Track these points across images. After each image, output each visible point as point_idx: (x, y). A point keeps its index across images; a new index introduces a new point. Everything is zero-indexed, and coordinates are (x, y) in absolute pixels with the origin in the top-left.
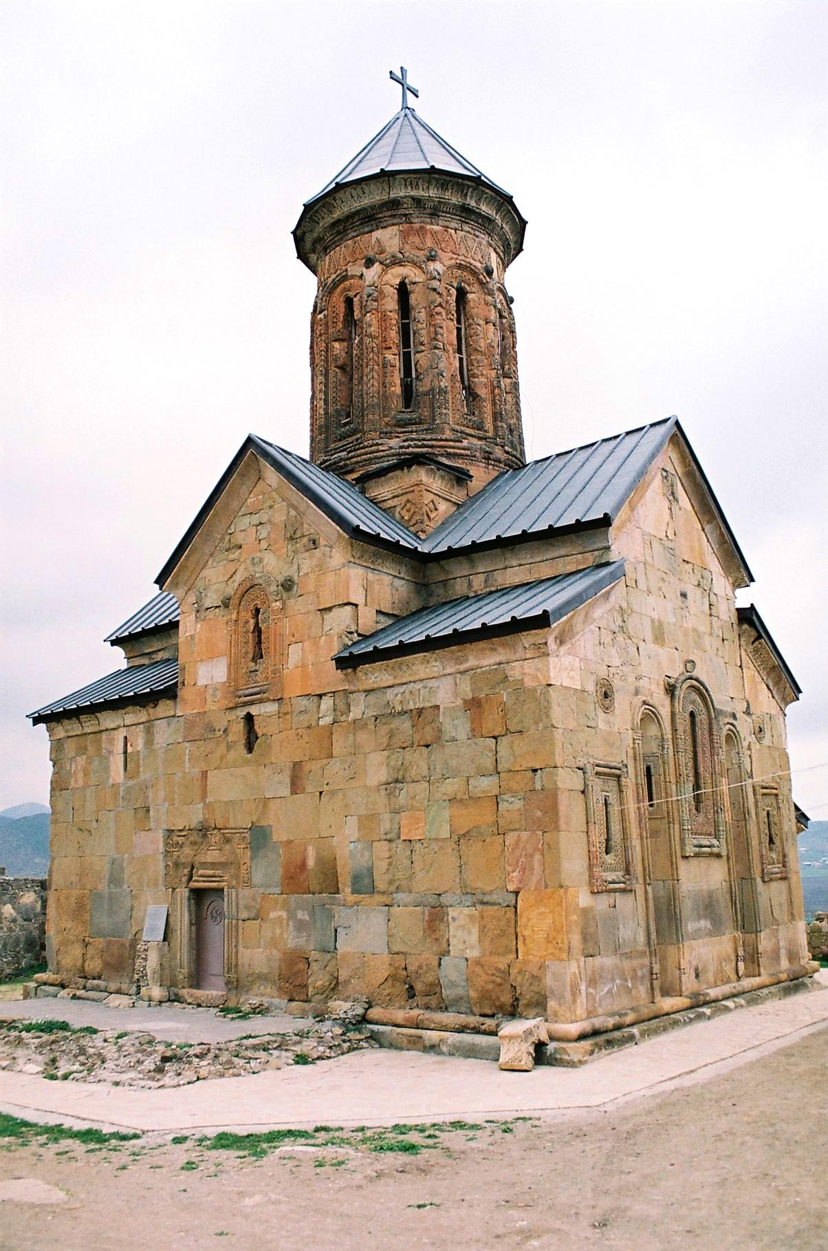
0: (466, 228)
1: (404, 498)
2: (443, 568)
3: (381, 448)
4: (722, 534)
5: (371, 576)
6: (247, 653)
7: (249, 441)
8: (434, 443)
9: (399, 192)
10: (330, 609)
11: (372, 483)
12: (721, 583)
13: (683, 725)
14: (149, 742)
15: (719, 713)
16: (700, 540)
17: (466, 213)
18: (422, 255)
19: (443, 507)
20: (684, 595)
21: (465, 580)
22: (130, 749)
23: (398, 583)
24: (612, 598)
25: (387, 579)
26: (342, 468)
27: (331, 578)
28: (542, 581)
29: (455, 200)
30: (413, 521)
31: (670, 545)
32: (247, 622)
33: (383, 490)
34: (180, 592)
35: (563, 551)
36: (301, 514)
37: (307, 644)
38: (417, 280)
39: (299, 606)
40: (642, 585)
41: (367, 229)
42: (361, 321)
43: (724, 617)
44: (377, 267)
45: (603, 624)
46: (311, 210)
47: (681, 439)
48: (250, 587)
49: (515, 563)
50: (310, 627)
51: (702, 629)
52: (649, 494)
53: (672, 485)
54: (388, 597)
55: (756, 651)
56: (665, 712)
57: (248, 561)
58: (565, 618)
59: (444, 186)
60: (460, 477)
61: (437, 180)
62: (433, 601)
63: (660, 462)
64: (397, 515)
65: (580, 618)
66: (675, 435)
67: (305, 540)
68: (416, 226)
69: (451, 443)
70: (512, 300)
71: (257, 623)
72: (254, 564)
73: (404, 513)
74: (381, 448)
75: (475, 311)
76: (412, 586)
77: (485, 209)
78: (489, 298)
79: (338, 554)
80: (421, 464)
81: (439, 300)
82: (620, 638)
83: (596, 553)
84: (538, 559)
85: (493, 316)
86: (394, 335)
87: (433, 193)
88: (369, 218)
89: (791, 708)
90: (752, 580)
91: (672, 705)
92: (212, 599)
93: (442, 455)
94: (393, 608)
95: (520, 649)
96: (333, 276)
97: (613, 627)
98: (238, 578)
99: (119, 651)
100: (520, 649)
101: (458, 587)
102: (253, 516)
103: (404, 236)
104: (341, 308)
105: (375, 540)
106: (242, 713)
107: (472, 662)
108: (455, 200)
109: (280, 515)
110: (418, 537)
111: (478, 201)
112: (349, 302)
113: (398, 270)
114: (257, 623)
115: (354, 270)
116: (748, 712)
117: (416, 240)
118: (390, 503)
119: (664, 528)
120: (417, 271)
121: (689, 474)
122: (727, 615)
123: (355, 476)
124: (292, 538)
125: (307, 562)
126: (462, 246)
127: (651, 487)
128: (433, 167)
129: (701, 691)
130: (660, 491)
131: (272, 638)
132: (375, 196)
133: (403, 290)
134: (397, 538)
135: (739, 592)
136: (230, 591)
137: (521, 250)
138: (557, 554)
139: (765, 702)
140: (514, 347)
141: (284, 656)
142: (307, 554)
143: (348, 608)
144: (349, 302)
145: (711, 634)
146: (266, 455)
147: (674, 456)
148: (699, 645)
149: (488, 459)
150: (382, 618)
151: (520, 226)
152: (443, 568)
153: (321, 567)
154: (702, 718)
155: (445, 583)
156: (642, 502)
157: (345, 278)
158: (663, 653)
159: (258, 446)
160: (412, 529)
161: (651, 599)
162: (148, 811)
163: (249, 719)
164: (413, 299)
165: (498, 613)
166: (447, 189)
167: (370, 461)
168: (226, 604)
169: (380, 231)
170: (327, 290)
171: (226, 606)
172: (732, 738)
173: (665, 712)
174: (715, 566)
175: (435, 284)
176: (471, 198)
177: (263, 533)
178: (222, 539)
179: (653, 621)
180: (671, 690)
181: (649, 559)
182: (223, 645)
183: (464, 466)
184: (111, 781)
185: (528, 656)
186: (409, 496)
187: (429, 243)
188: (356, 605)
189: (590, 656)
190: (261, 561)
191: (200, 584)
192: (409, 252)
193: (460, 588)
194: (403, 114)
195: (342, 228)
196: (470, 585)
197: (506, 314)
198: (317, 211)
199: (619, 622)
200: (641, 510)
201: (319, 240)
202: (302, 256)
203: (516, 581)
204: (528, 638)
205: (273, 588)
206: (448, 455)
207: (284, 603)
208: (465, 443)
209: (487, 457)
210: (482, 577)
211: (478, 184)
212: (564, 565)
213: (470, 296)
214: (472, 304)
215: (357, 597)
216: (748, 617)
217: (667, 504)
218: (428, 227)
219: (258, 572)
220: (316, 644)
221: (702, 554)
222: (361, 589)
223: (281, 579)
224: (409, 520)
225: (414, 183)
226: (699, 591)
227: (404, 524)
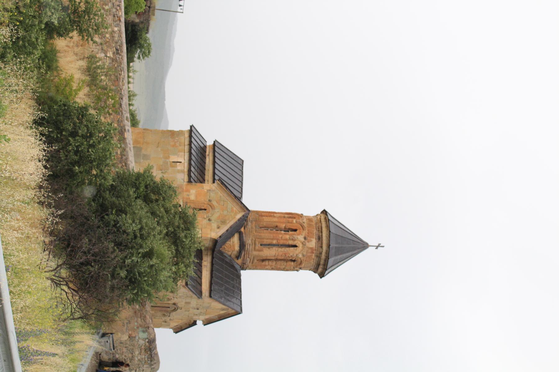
13: (167, 305)
14: (179, 171)
15: (170, 313)
18: (305, 253)
22: (178, 164)
44: (303, 240)
48: (212, 207)
55: (186, 324)
56: (170, 302)
59: (325, 261)
86: (281, 242)
89: (171, 330)
99: (212, 143)
103: (311, 248)
108: (322, 262)
112: (295, 230)
116: (170, 320)
117: (310, 251)
120: (300, 251)
121: (229, 314)
122: (195, 318)
125: (214, 225)
129: (175, 310)
139: (174, 324)
144: (295, 230)
154: (169, 309)
155: (207, 255)
157: (303, 229)
158: (183, 303)
164: (292, 249)
172: (164, 315)
173: (170, 302)
180: (174, 304)
184: (170, 156)
216: (194, 323)
219: (216, 210)
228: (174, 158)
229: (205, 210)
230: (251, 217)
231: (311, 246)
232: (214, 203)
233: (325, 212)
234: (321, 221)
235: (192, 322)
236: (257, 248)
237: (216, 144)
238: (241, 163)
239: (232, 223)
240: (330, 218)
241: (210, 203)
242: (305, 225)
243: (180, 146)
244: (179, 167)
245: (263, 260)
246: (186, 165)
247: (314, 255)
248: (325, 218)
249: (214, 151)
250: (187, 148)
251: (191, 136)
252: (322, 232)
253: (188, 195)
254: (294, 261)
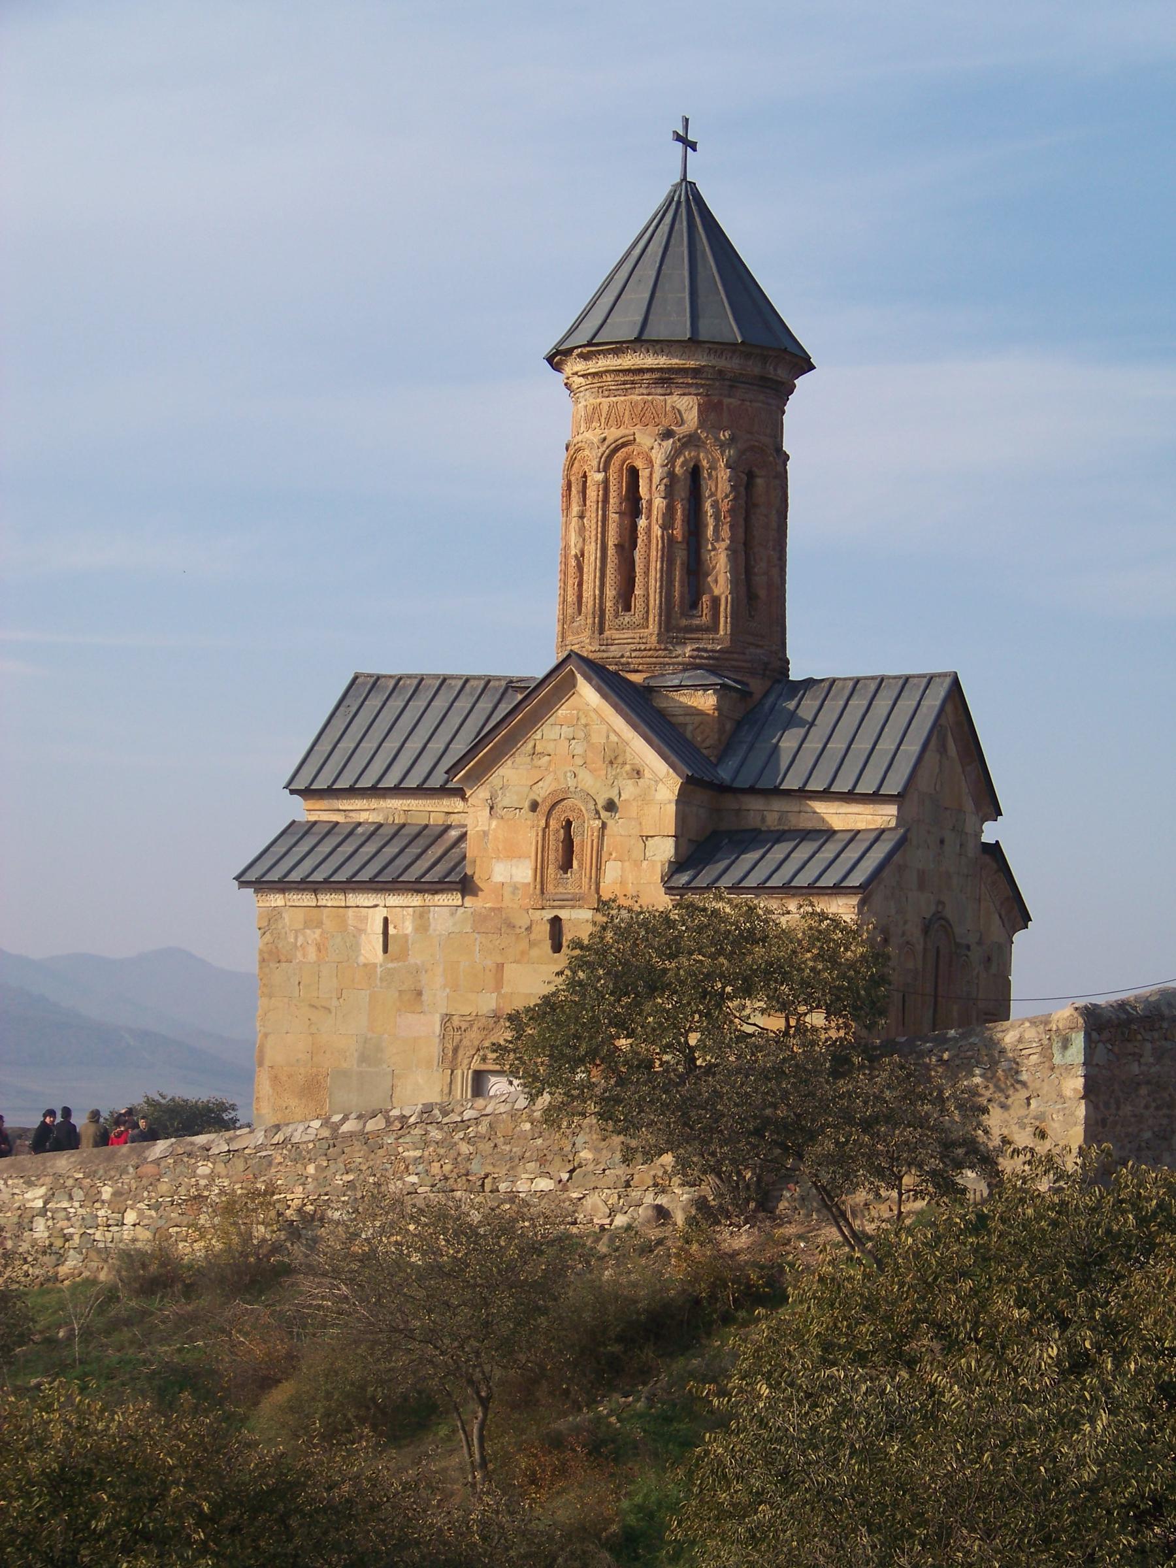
0: (761, 397)
15: (958, 945)
20: (942, 842)
22: (391, 931)
56: (919, 948)
89: (1018, 937)
91: (925, 943)
106: (549, 914)
117: (712, 416)
122: (972, 851)
125: (629, 790)
135: (987, 826)
162: (420, 994)
163: (556, 922)
174: (969, 806)
180: (926, 930)
184: (362, 960)
196: (763, 820)
210: (776, 816)
216: (995, 850)
228: (371, 949)
229: (569, 823)
230: (585, 643)
232: (542, 792)
233: (556, 359)
234: (594, 374)
235: (987, 859)
237: (300, 784)
238: (363, 689)
239: (619, 723)
240: (582, 337)
241: (543, 808)
242: (613, 433)
243: (320, 924)
244: (404, 926)
245: (751, 596)
246: (393, 900)
247: (726, 401)
248: (585, 357)
249: (330, 792)
250: (327, 899)
251: (283, 886)
252: (641, 371)
253: (515, 888)
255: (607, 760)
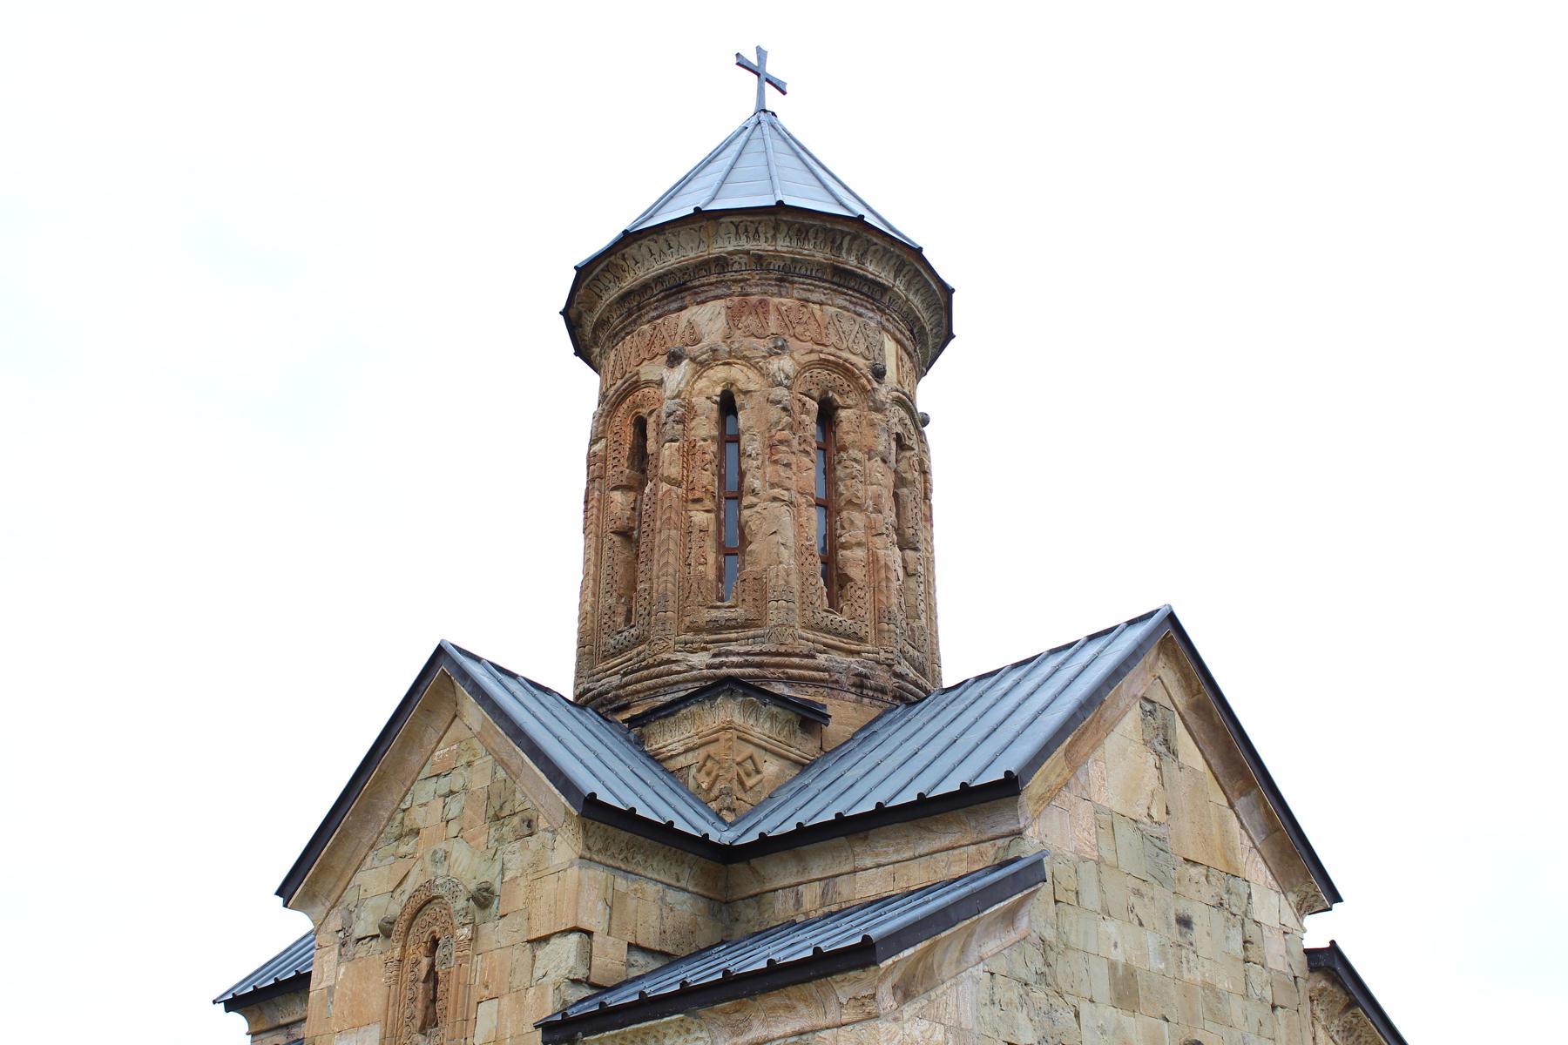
0: (840, 301)
1: (702, 753)
2: (754, 871)
3: (675, 667)
4: (1269, 814)
5: (622, 884)
6: (412, 1017)
7: (440, 651)
8: (765, 659)
9: (725, 245)
10: (545, 939)
11: (654, 727)
12: (1269, 903)
16: (1223, 823)
17: (842, 279)
18: (763, 345)
19: (771, 767)
20: (1185, 922)
21: (791, 895)
23: (673, 897)
24: (1023, 924)
25: (652, 889)
26: (611, 701)
27: (549, 886)
28: (913, 892)
29: (821, 255)
30: (715, 792)
31: (1158, 831)
32: (417, 963)
33: (671, 739)
34: (320, 910)
35: (946, 841)
36: (513, 775)
37: (505, 1001)
38: (752, 387)
39: (499, 935)
40: (1091, 899)
41: (674, 305)
42: (657, 455)
43: (1277, 962)
45: (999, 966)
46: (588, 274)
47: (1181, 647)
48: (425, 903)
49: (868, 862)
50: (512, 972)
51: (1224, 984)
52: (1113, 743)
53: (1165, 727)
54: (653, 920)
55: (1349, 1030)
57: (428, 858)
58: (910, 951)
59: (802, 233)
60: (810, 718)
61: (790, 225)
62: (740, 930)
63: (1135, 684)
64: (692, 784)
65: (953, 954)
66: (1167, 640)
67: (516, 820)
68: (754, 299)
69: (796, 660)
70: (925, 421)
71: (432, 966)
72: (435, 862)
73: (702, 777)
74: (675, 667)
75: (848, 439)
76: (701, 904)
77: (872, 269)
78: (877, 417)
79: (564, 846)
80: (732, 694)
81: (786, 419)
82: (1039, 995)
83: (1000, 843)
84: (908, 854)
85: (884, 443)
87: (783, 246)
88: (678, 288)
90: (1336, 897)
92: (366, 924)
93: (779, 680)
94: (663, 940)
95: (833, 1007)
96: (619, 382)
97: (1023, 973)
98: (409, 887)
100: (833, 1007)
101: (778, 906)
102: (442, 780)
103: (734, 316)
104: (628, 433)
105: (627, 819)
107: (757, 1032)
109: (480, 778)
110: (722, 820)
111: (861, 258)
112: (640, 425)
113: (719, 372)
114: (432, 966)
115: (649, 371)
117: (750, 321)
118: (681, 762)
119: (1144, 802)
120: (752, 374)
121: (1199, 708)
123: (627, 715)
124: (497, 818)
125: (517, 858)
126: (832, 331)
127: (1118, 729)
128: (780, 203)
130: (1137, 737)
131: (452, 990)
132: (688, 252)
133: (728, 405)
134: (669, 815)
135: (1309, 921)
136: (395, 909)
137: (950, 336)
138: (936, 845)
140: (926, 497)
141: (468, 1020)
142: (517, 844)
143: (574, 937)
145: (1246, 996)
146: (465, 676)
147: (1170, 676)
148: (1218, 1017)
149: (861, 686)
150: (639, 958)
151: (941, 297)
152: (754, 871)
153: (536, 868)
156: (1099, 752)
157: (635, 386)
159: (454, 662)
160: (714, 805)
161: (1111, 928)
165: (796, 948)
166: (806, 238)
167: (654, 691)
168: (386, 931)
169: (694, 309)
170: (611, 404)
171: (388, 936)
175: (780, 392)
176: (849, 252)
177: (454, 808)
178: (390, 819)
179: (1113, 966)
181: (1109, 856)
182: (376, 1003)
183: (819, 699)
185: (845, 1019)
186: (711, 749)
187: (773, 325)
188: (589, 933)
189: (968, 1021)
190: (446, 856)
191: (350, 897)
192: (741, 341)
193: (782, 907)
194: (754, 120)
195: (636, 303)
196: (798, 902)
197: (913, 442)
198: (597, 279)
199: (1039, 964)
200: (1093, 769)
201: (601, 324)
202: (582, 351)
203: (871, 892)
204: (845, 988)
205: (461, 903)
206: (790, 680)
207: (475, 930)
208: (821, 659)
209: (861, 684)
210: (817, 888)
211: (856, 231)
212: (949, 865)
213: (843, 414)
214: (845, 426)
215: (594, 919)
216: (1329, 964)
217: (1152, 760)
218: (776, 300)
220: (519, 1001)
221: (1227, 848)
222: (600, 906)
223: (472, 887)
224: (710, 789)
225: (751, 230)
226: (1218, 917)
227: (700, 799)
231: (721, 323)
236: (739, 613)
241: (400, 927)
254: (827, 415)
255: (491, 813)
